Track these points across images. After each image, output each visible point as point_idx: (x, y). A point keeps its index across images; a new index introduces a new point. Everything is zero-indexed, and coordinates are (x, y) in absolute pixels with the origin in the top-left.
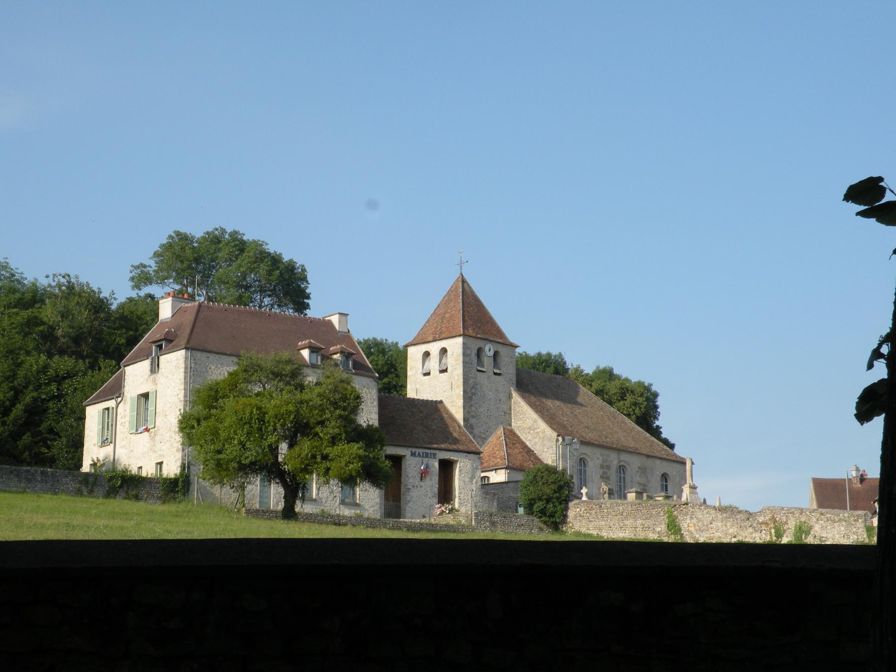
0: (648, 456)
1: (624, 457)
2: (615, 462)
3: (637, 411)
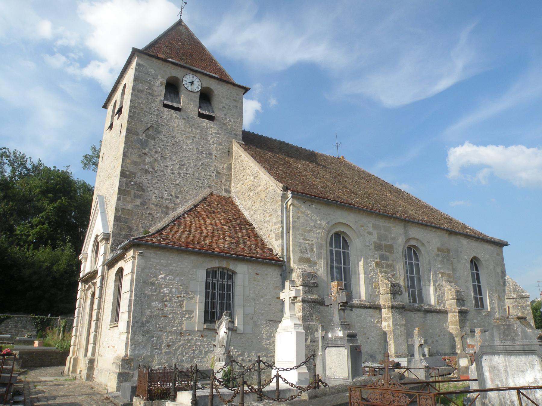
1: (415, 232)
2: (401, 240)
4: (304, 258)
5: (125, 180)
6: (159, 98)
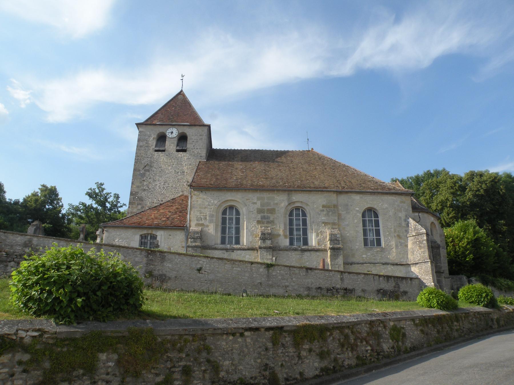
0: (339, 193)
1: (298, 198)
2: (284, 204)
3: (484, 186)
4: (199, 224)
5: (132, 197)
6: (152, 147)
